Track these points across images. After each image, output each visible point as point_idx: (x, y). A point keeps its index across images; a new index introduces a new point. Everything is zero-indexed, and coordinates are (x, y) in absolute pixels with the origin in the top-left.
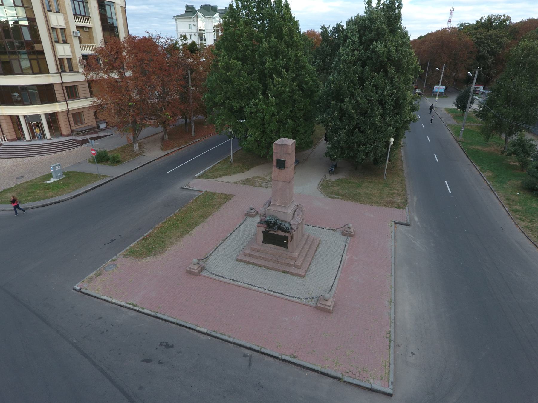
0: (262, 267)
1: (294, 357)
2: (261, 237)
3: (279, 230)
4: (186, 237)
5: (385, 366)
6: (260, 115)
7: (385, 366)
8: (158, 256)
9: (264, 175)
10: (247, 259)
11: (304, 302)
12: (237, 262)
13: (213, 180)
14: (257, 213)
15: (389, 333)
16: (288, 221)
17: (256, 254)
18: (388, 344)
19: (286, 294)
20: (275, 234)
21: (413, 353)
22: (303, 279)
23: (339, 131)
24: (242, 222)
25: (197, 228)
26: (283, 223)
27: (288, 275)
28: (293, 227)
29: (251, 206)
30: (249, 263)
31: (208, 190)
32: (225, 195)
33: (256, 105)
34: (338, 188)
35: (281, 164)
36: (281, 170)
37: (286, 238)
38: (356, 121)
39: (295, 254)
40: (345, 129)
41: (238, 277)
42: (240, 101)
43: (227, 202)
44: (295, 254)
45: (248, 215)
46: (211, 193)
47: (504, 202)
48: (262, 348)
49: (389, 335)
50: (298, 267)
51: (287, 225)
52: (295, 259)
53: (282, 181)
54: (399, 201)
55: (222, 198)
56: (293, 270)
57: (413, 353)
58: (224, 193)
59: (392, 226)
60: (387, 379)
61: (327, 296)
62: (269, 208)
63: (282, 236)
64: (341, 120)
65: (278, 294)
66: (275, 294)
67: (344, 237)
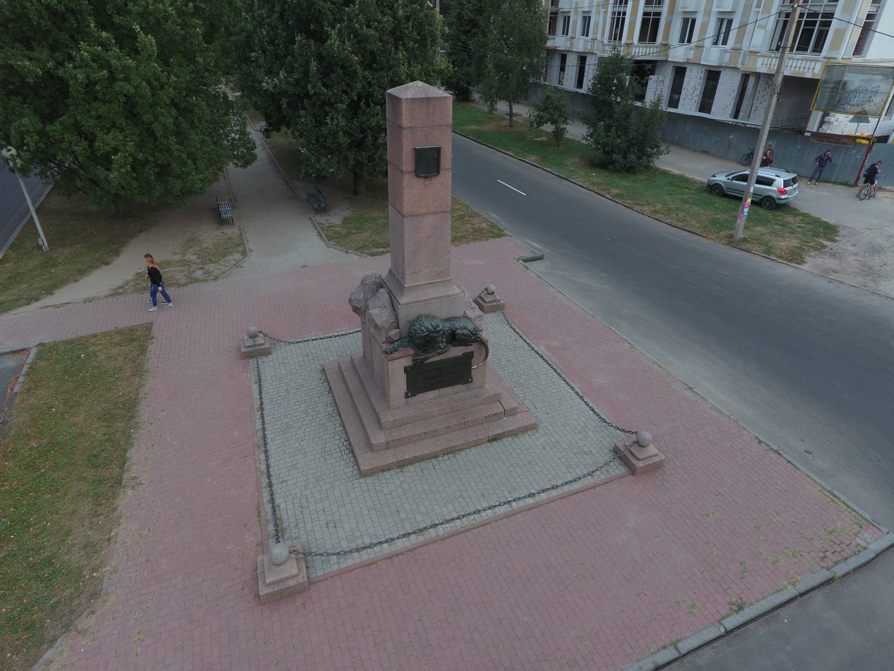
0: (436, 457)
1: (740, 608)
2: (399, 383)
3: (449, 346)
4: (125, 499)
5: (833, 501)
6: (119, 85)
7: (833, 501)
8: (87, 622)
9: (174, 253)
10: (391, 457)
11: (603, 477)
12: (369, 480)
13: (27, 308)
14: (275, 341)
15: (760, 442)
16: (460, 314)
17: (405, 432)
18: (786, 462)
19: (554, 483)
20: (441, 358)
21: (810, 453)
22: (540, 430)
23: (327, 108)
24: (253, 377)
25: (132, 453)
26: (458, 325)
27: (507, 441)
28: (477, 323)
29: (253, 329)
30: (401, 465)
31: (47, 338)
32: (119, 332)
33: (95, 58)
34: (365, 234)
35: (428, 163)
36: (427, 182)
37: (469, 356)
38: (360, 81)
39: (491, 388)
40: (343, 102)
41: (419, 518)
42: (32, 54)
43: (151, 347)
44: (491, 388)
45: (254, 352)
46: (66, 343)
47: (595, 188)
48: (675, 644)
49: (763, 444)
50: (511, 413)
51: (470, 327)
52: (497, 398)
53: (434, 213)
54: (484, 225)
55: (119, 345)
56: (509, 424)
57: (810, 453)
58: (113, 328)
59: (527, 268)
60: (864, 521)
61: (647, 435)
62: (403, 300)
63: (456, 359)
64: (326, 86)
65: (543, 496)
66: (538, 498)
67: (490, 315)
